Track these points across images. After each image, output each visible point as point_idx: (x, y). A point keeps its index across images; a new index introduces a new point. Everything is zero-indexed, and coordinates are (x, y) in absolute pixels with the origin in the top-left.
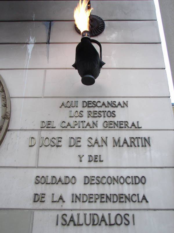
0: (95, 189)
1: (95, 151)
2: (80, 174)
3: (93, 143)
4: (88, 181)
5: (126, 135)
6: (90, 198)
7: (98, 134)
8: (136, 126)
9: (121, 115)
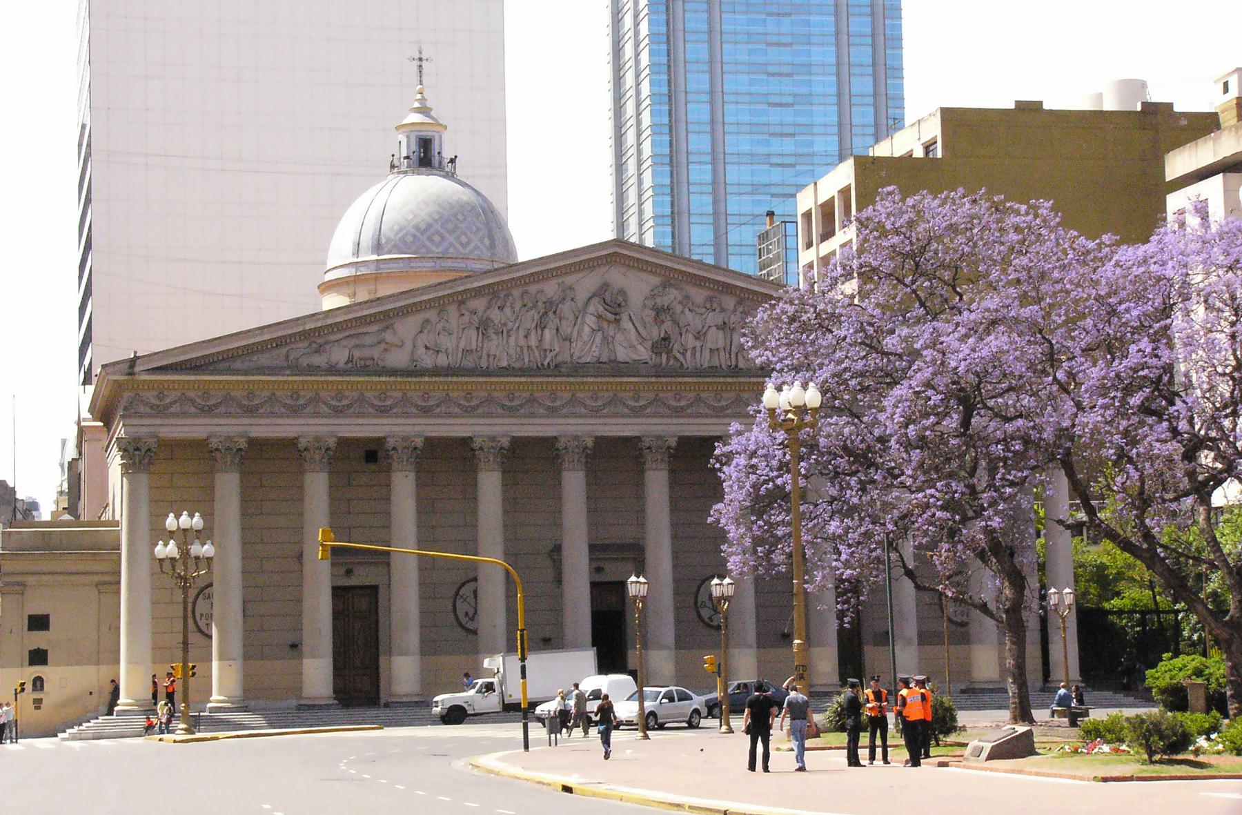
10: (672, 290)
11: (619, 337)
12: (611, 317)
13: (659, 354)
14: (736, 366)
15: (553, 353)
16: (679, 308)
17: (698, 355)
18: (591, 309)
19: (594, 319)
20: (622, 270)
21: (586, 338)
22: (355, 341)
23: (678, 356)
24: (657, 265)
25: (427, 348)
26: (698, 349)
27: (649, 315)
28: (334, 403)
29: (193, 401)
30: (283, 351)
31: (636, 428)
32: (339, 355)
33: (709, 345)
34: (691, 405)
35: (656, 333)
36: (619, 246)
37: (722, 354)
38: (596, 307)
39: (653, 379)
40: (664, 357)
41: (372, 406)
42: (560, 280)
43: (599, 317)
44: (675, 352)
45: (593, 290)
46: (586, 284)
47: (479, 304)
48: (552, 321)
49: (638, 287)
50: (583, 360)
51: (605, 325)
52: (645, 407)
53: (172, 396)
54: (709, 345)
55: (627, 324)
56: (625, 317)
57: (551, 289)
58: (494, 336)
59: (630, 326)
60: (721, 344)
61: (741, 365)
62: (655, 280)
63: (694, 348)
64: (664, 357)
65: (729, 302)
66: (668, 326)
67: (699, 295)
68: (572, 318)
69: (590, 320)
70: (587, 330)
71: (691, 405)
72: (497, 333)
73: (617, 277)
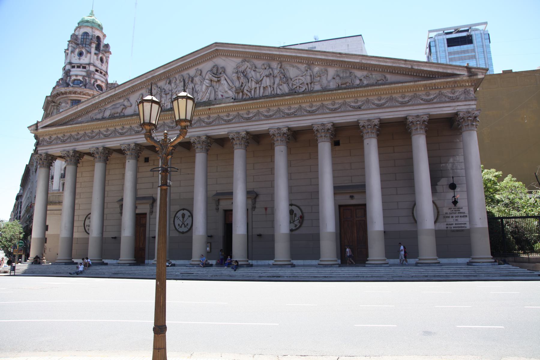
0: (457, 226)
1: (457, 218)
2: (454, 223)
3: (456, 217)
4: (456, 224)
5: (462, 215)
6: (456, 227)
7: (457, 215)
8: (464, 213)
9: (461, 211)
10: (246, 63)
11: (220, 88)
12: (216, 79)
16: (248, 70)
18: (207, 77)
19: (207, 81)
20: (224, 58)
21: (204, 90)
22: (114, 107)
24: (237, 52)
26: (258, 88)
27: (235, 75)
28: (105, 133)
29: (60, 138)
30: (90, 115)
31: (226, 130)
32: (107, 114)
33: (262, 85)
34: (254, 116)
35: (237, 84)
36: (216, 46)
38: (209, 76)
39: (232, 104)
41: (119, 133)
42: (196, 68)
43: (211, 81)
44: (245, 91)
45: (210, 69)
46: (206, 66)
47: (161, 84)
48: (191, 86)
49: (230, 65)
50: (202, 101)
51: (214, 84)
52: (232, 119)
53: (54, 137)
55: (223, 82)
56: (222, 79)
57: (192, 72)
58: (164, 96)
59: (225, 82)
60: (268, 84)
61: (278, 93)
62: (239, 60)
63: (256, 88)
65: (274, 65)
66: (242, 79)
67: (259, 63)
68: (199, 83)
69: (207, 82)
70: (204, 87)
71: (254, 116)
72: (166, 94)
73: (220, 61)
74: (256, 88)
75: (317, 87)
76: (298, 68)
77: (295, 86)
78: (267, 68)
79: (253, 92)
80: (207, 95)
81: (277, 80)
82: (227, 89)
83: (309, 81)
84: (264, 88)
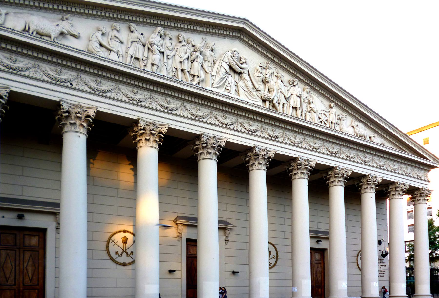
13: (264, 101)
14: (305, 120)
15: (200, 79)
17: (285, 108)
23: (277, 105)
25: (101, 45)
26: (285, 105)
37: (299, 112)
40: (267, 103)
44: (274, 102)
54: (292, 104)
63: (284, 104)
64: (267, 103)
69: (227, 68)
74: (284, 104)
75: (338, 129)
76: (322, 102)
77: (321, 120)
78: (297, 87)
79: (281, 105)
80: (226, 84)
81: (305, 106)
82: (252, 89)
83: (334, 121)
84: (293, 108)
